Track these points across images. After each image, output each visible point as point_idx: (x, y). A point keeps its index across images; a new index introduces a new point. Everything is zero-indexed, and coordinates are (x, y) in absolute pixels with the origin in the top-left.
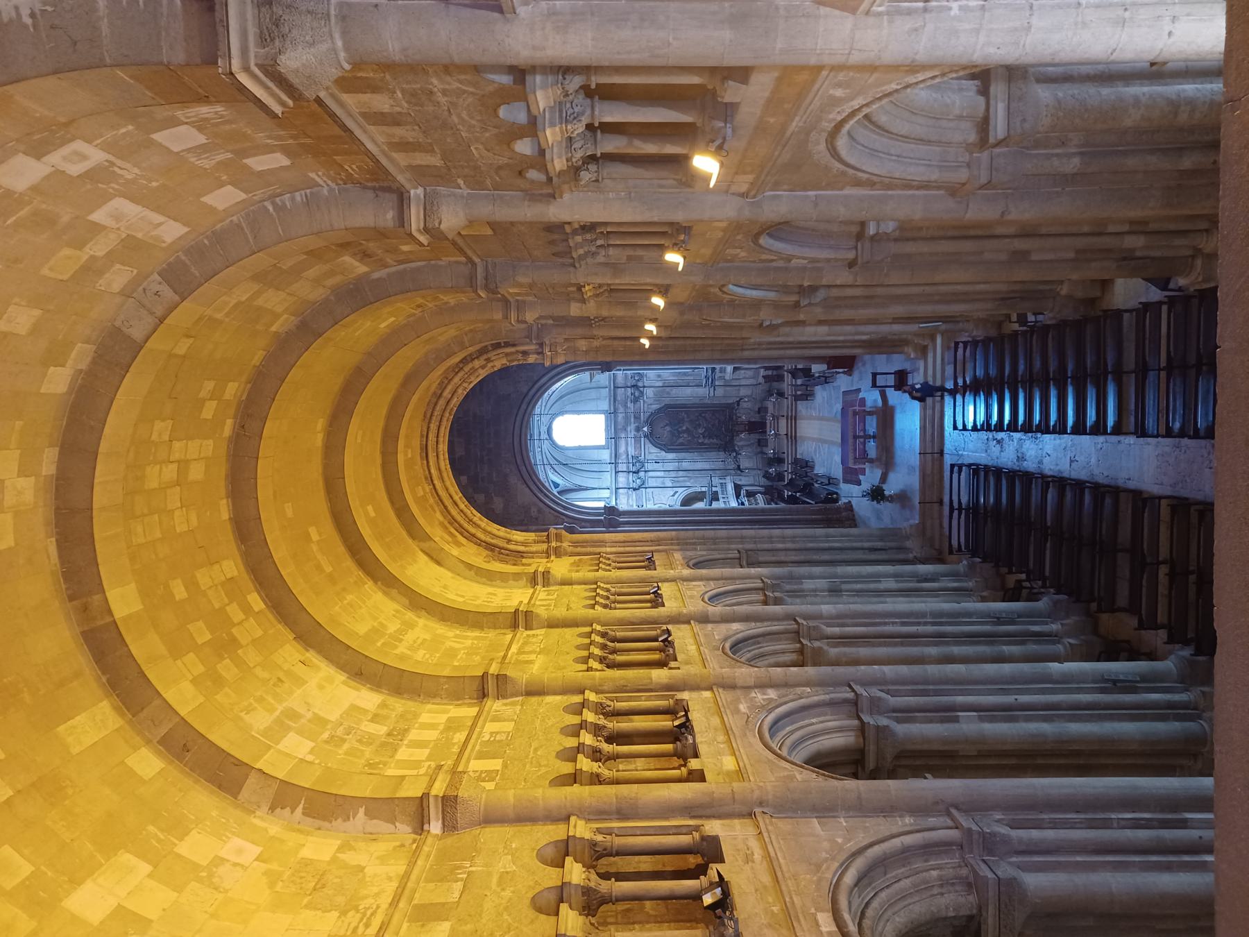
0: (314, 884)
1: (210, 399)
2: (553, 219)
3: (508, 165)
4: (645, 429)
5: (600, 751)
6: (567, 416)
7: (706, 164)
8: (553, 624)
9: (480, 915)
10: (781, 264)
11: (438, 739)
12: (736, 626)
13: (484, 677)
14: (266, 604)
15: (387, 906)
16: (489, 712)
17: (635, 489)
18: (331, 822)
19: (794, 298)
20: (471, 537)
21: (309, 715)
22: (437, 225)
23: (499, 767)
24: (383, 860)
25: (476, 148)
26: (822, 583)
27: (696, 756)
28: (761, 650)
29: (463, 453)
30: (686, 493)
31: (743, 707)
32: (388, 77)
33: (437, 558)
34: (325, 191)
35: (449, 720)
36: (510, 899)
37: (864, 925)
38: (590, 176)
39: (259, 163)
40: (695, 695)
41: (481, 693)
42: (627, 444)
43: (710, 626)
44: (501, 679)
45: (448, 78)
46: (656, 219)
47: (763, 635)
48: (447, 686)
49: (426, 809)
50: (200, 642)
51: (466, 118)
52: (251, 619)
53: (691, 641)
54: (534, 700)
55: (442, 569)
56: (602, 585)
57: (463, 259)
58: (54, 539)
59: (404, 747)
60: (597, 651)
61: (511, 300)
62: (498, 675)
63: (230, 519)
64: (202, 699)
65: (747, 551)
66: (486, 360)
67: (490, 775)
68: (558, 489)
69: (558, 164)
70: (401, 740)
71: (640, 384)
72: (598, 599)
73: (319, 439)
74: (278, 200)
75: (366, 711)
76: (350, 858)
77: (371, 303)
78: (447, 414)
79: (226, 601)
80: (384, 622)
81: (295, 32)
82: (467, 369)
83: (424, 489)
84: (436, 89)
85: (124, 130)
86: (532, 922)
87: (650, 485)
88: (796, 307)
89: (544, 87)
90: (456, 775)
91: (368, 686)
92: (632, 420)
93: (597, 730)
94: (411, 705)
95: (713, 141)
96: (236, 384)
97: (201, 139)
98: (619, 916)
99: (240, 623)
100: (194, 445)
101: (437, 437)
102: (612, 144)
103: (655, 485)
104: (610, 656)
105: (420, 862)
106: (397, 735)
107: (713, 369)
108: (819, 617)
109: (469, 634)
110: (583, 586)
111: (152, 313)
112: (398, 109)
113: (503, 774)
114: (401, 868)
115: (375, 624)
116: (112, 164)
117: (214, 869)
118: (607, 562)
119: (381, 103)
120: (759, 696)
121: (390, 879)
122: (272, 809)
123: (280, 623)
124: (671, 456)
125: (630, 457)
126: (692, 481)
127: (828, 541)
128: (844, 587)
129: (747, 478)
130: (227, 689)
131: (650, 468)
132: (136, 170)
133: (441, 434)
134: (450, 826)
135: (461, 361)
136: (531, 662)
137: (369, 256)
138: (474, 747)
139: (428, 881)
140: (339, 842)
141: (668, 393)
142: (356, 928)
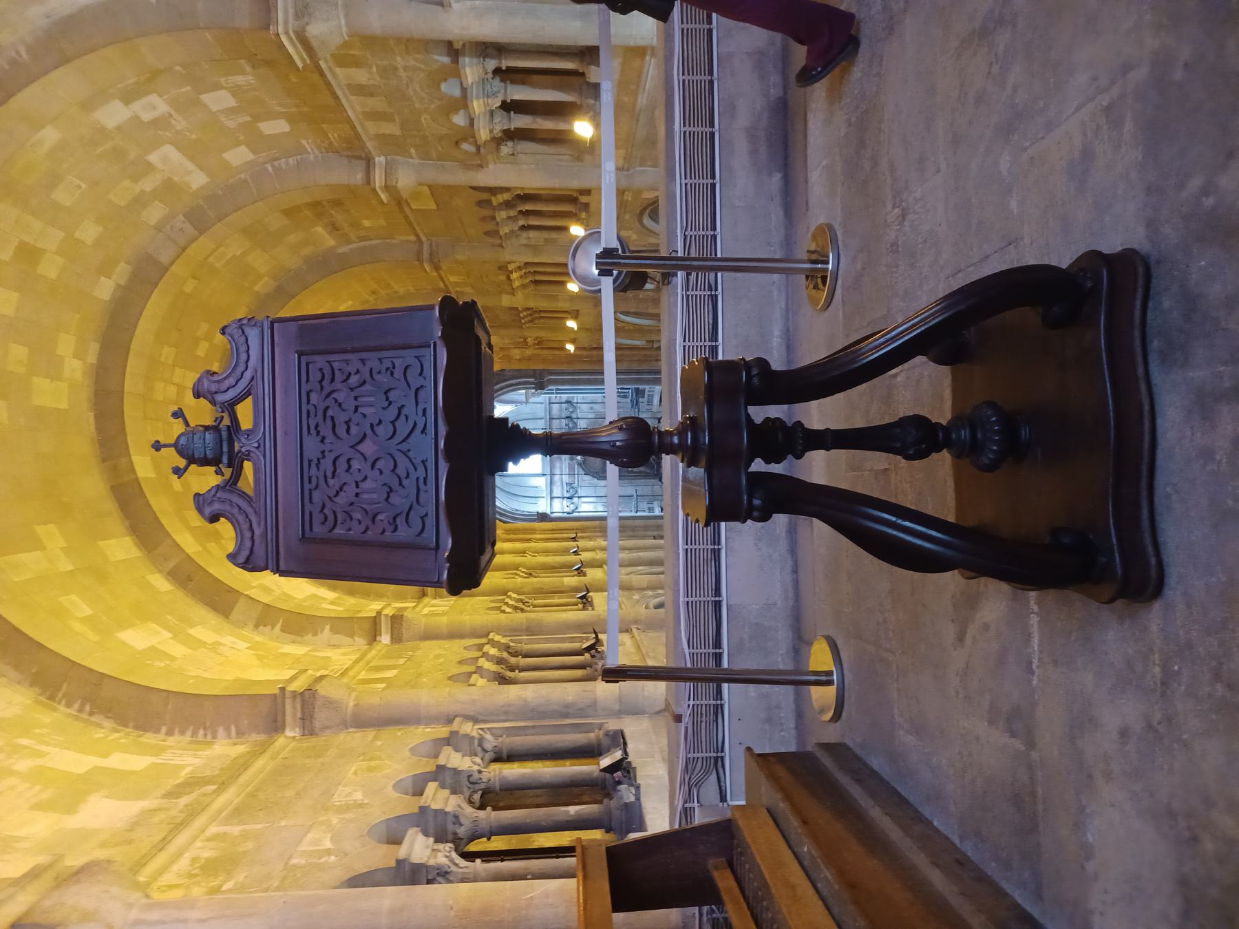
21: (279, 592)
25: (425, 119)
34: (312, 157)
41: (421, 593)
51: (419, 91)
57: (413, 238)
58: (93, 414)
69: (483, 134)
71: (574, 416)
74: (276, 163)
77: (336, 272)
84: (399, 66)
85: (183, 90)
89: (471, 65)
97: (232, 102)
102: (521, 121)
107: (639, 393)
112: (372, 82)
116: (171, 115)
119: (361, 76)
126: (622, 506)
131: (583, 494)
132: (184, 123)
134: (396, 638)
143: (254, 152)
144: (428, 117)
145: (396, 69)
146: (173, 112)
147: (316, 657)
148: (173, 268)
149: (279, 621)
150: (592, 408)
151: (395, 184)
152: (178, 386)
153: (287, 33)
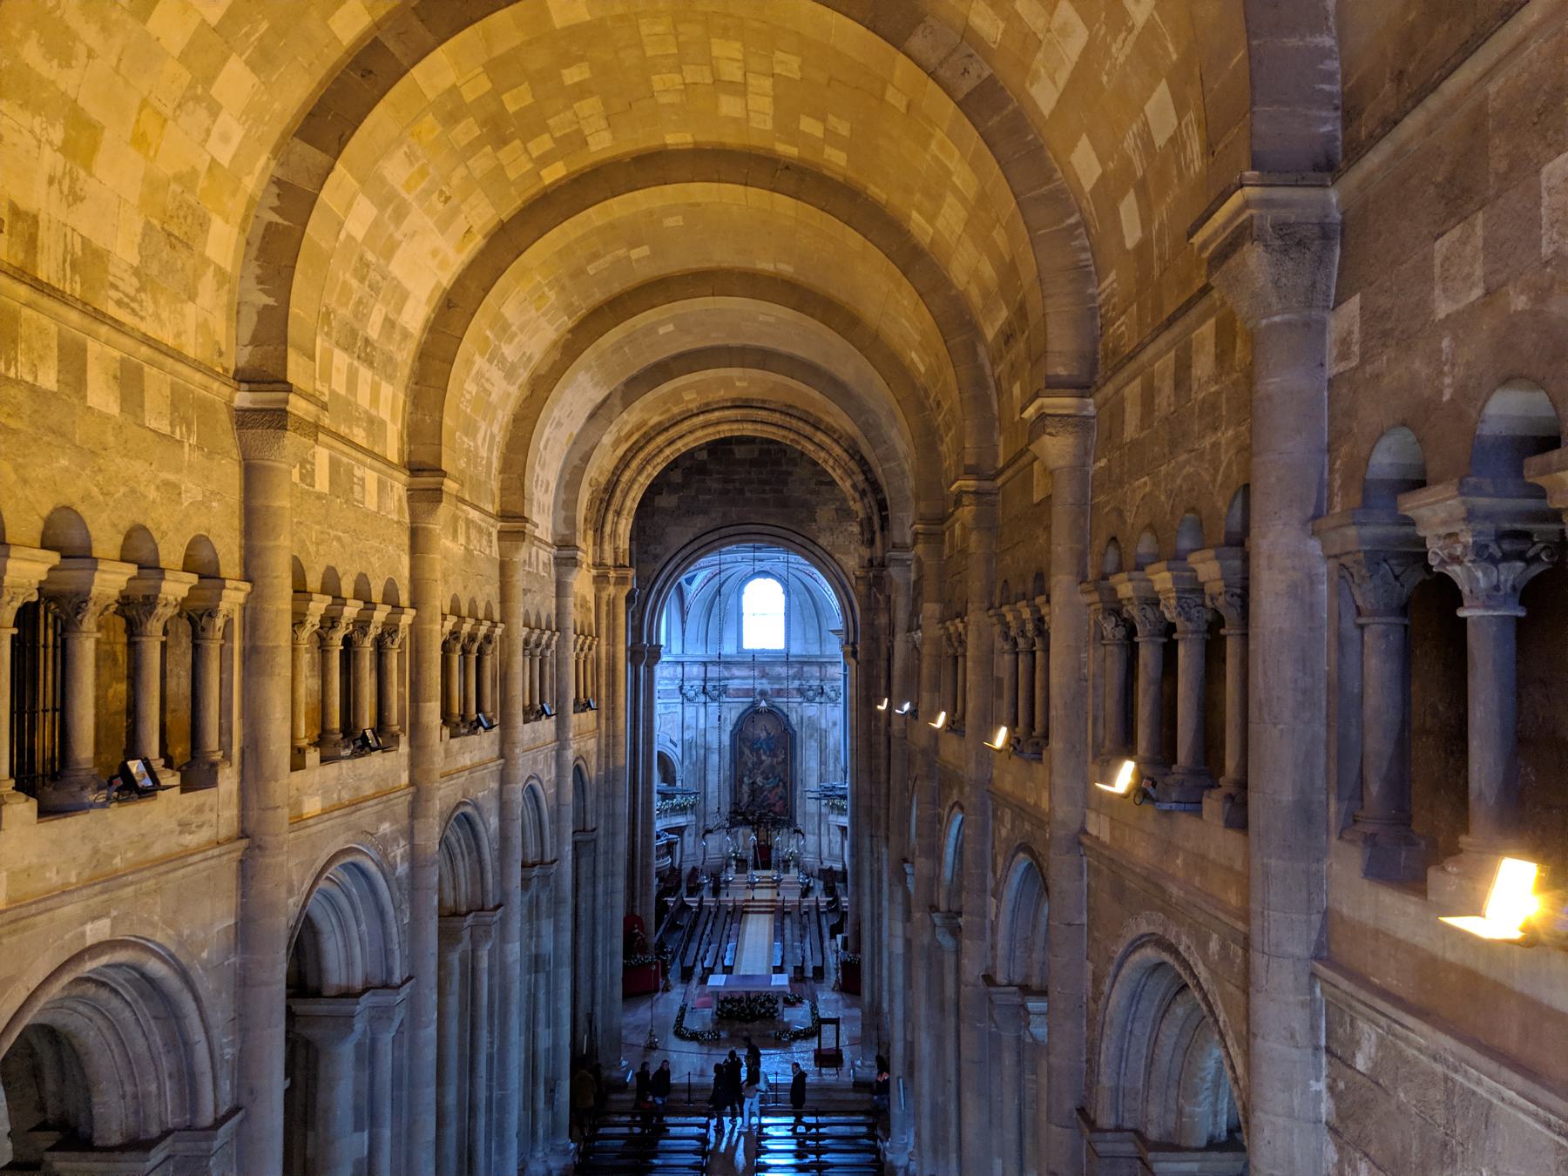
0: (177, 234)
1: (826, 130)
2: (1053, 581)
3: (1125, 522)
4: (763, 704)
5: (333, 627)
6: (783, 597)
7: (1125, 776)
8: (505, 568)
9: (125, 455)
10: (990, 883)
11: (357, 406)
12: (494, 822)
13: (438, 471)
14: (551, 185)
15: (143, 330)
16: (391, 477)
17: (681, 688)
18: (256, 259)
19: (943, 906)
20: (624, 462)
21: (398, 236)
22: (1048, 430)
23: (318, 487)
24: (203, 327)
26: (548, 945)
27: (324, 760)
28: (459, 857)
30: (674, 759)
31: (385, 827)
32: (1235, 375)
33: (599, 414)
35: (383, 423)
36: (145, 497)
37: (89, 985)
38: (1109, 628)
39: (1129, 208)
40: (405, 761)
41: (415, 467)
43: (494, 785)
44: (436, 495)
45: (1232, 451)
46: (1053, 713)
47: (480, 861)
49: (271, 387)
50: (504, 97)
51: (1185, 472)
52: (530, 166)
53: (476, 760)
54: (405, 540)
55: (583, 420)
56: (555, 638)
57: (1001, 464)
59: (348, 360)
60: (467, 628)
61: (945, 526)
62: (441, 490)
63: (666, 145)
64: (431, 96)
65: (595, 840)
67: (308, 476)
68: (684, 583)
72: (537, 631)
73: (765, 265)
75: (399, 311)
76: (207, 285)
77: (946, 342)
78: (792, 436)
79: (557, 135)
80: (516, 340)
81: (1289, 265)
82: (852, 465)
83: (694, 400)
84: (1219, 434)
85: (1171, 48)
86: (114, 525)
87: (686, 709)
88: (931, 907)
90: (314, 429)
91: (433, 316)
92: (777, 686)
93: (362, 624)
94: (404, 372)
95: (1154, 785)
96: (843, 164)
97: (1160, 140)
98: (108, 647)
99: (526, 149)
100: (766, 104)
101: (762, 422)
102: (1148, 656)
103: (687, 715)
104: (459, 647)
105: (198, 377)
106: (365, 352)
108: (504, 939)
109: (496, 454)
110: (554, 612)
111: (941, 65)
112: (1195, 387)
113: (309, 493)
114: (190, 352)
115: (514, 328)
116: (1130, 30)
117: (204, 105)
118: (586, 647)
119: (1203, 365)
120: (399, 851)
121: (178, 335)
122: (277, 182)
123: (524, 203)
124: (726, 740)
125: (726, 682)
127: (604, 956)
128: (542, 977)
129: (692, 843)
130: (440, 129)
131: (709, 709)
132: (1121, 59)
133: (765, 428)
134: (244, 419)
135: (862, 457)
136: (455, 537)
137: (1007, 343)
138: (347, 455)
139: (173, 386)
140: (229, 269)
141: (812, 736)
142: (116, 288)
143: (1093, 191)
144: (1148, 489)
145: (1216, 429)
146: (1136, 32)
147: (197, 277)
148: (901, 57)
149: (285, 219)
150: (835, 724)
151: (1048, 430)
152: (745, 84)
153: (1247, 204)
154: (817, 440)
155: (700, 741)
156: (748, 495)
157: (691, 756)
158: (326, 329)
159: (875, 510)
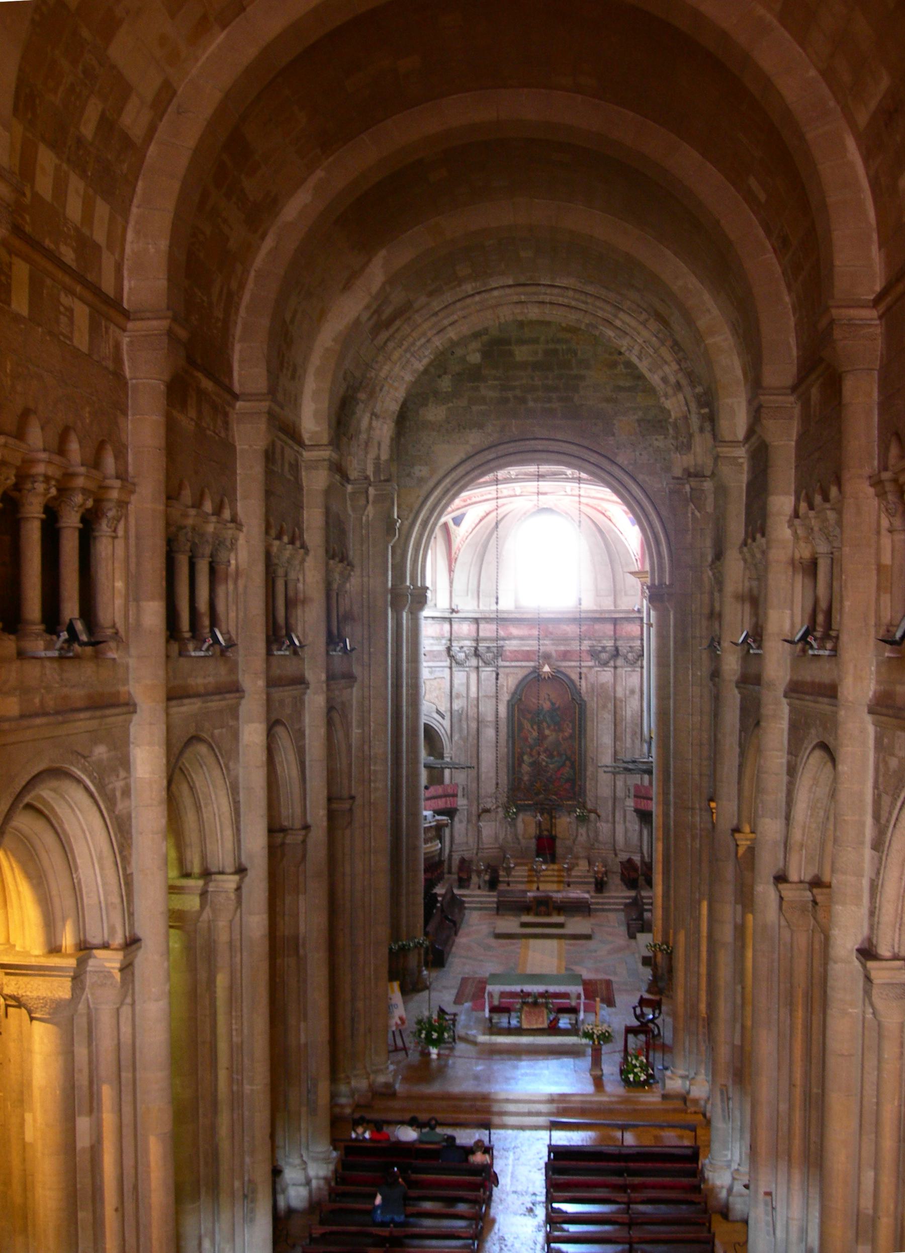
29: (518, 358)
30: (441, 732)
35: (99, 247)
42: (521, 638)
48: (152, 250)
59: (57, 161)
66: (678, 383)
70: (68, 159)
71: (620, 662)
82: (665, 352)
87: (455, 674)
92: (562, 648)
101: (551, 303)
103: (456, 682)
125: (501, 643)
131: (483, 675)
141: (604, 707)
150: (632, 692)
154: (618, 323)
155: (472, 712)
156: (531, 404)
157: (461, 730)
158: (30, 116)
159: (693, 406)
